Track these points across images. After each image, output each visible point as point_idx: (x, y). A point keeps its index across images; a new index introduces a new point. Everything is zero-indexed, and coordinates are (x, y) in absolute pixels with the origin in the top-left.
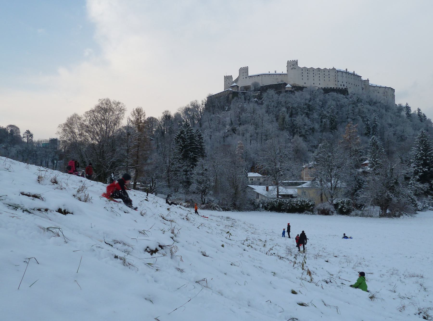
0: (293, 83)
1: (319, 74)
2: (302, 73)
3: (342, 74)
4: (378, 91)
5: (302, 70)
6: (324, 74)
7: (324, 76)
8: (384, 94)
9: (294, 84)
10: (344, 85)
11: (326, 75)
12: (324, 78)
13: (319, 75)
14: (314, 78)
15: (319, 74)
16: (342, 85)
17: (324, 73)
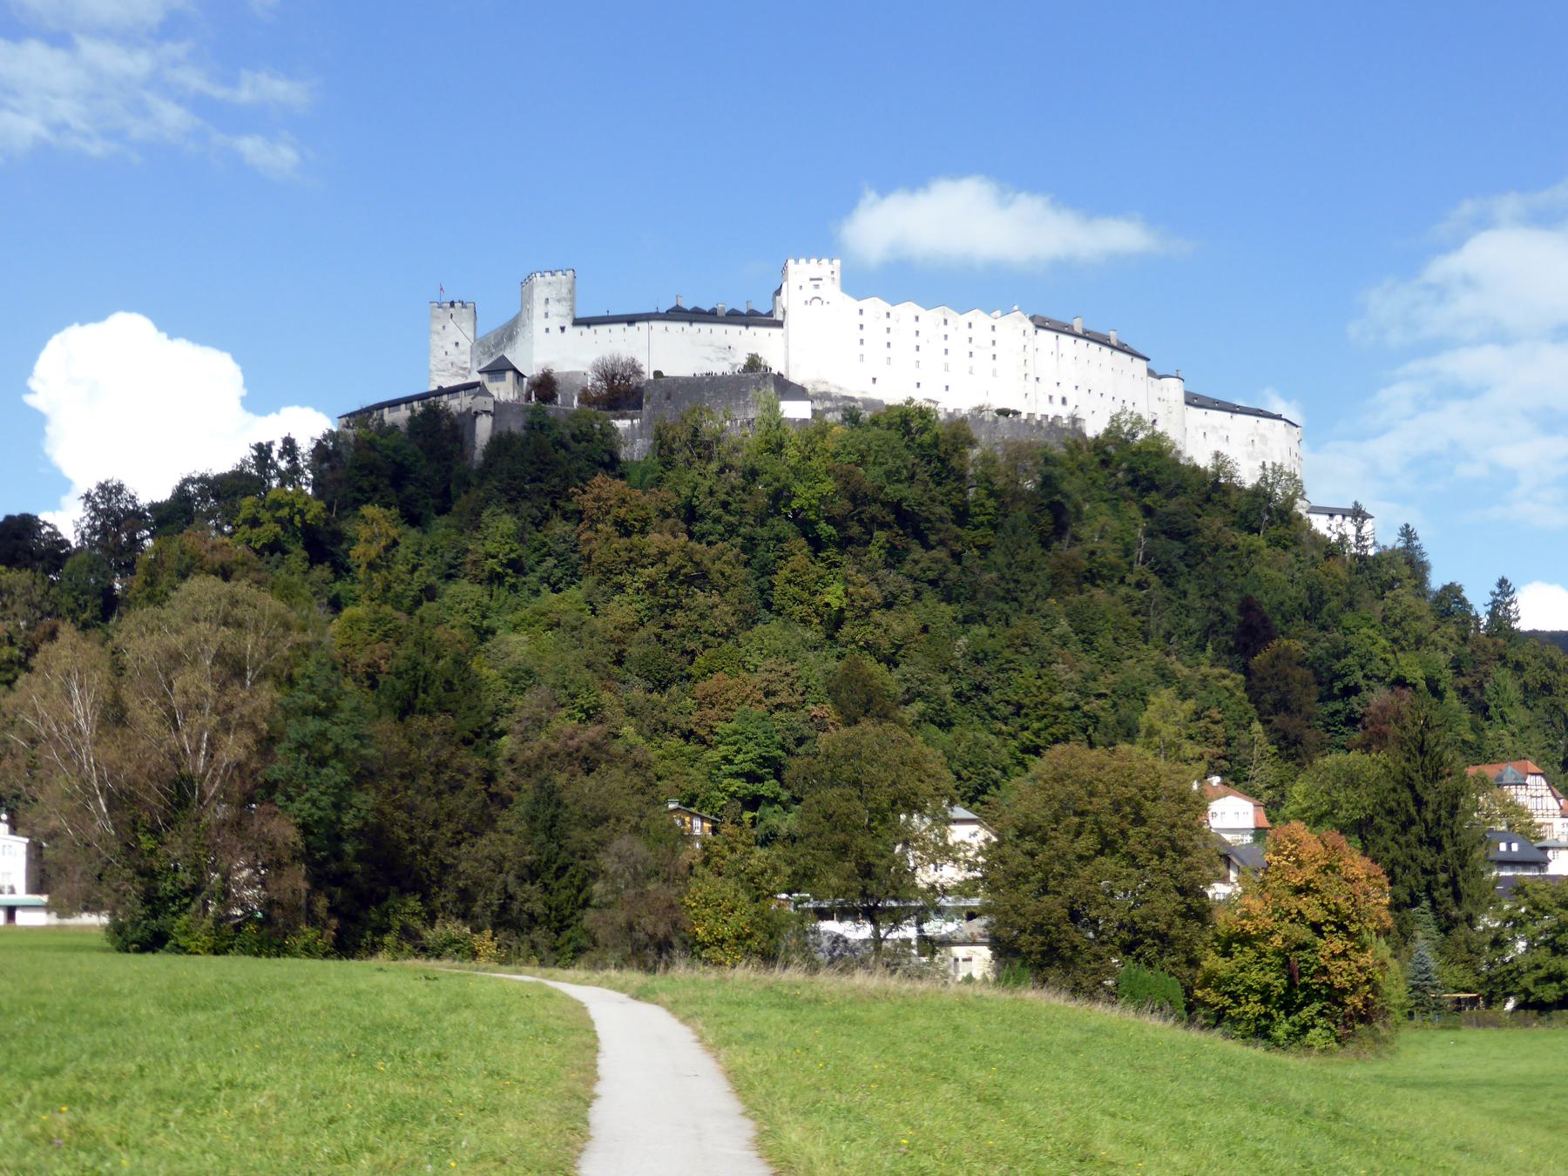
7: (971, 347)
8: (1250, 448)
9: (817, 382)
10: (1064, 401)
11: (978, 347)
16: (1057, 400)
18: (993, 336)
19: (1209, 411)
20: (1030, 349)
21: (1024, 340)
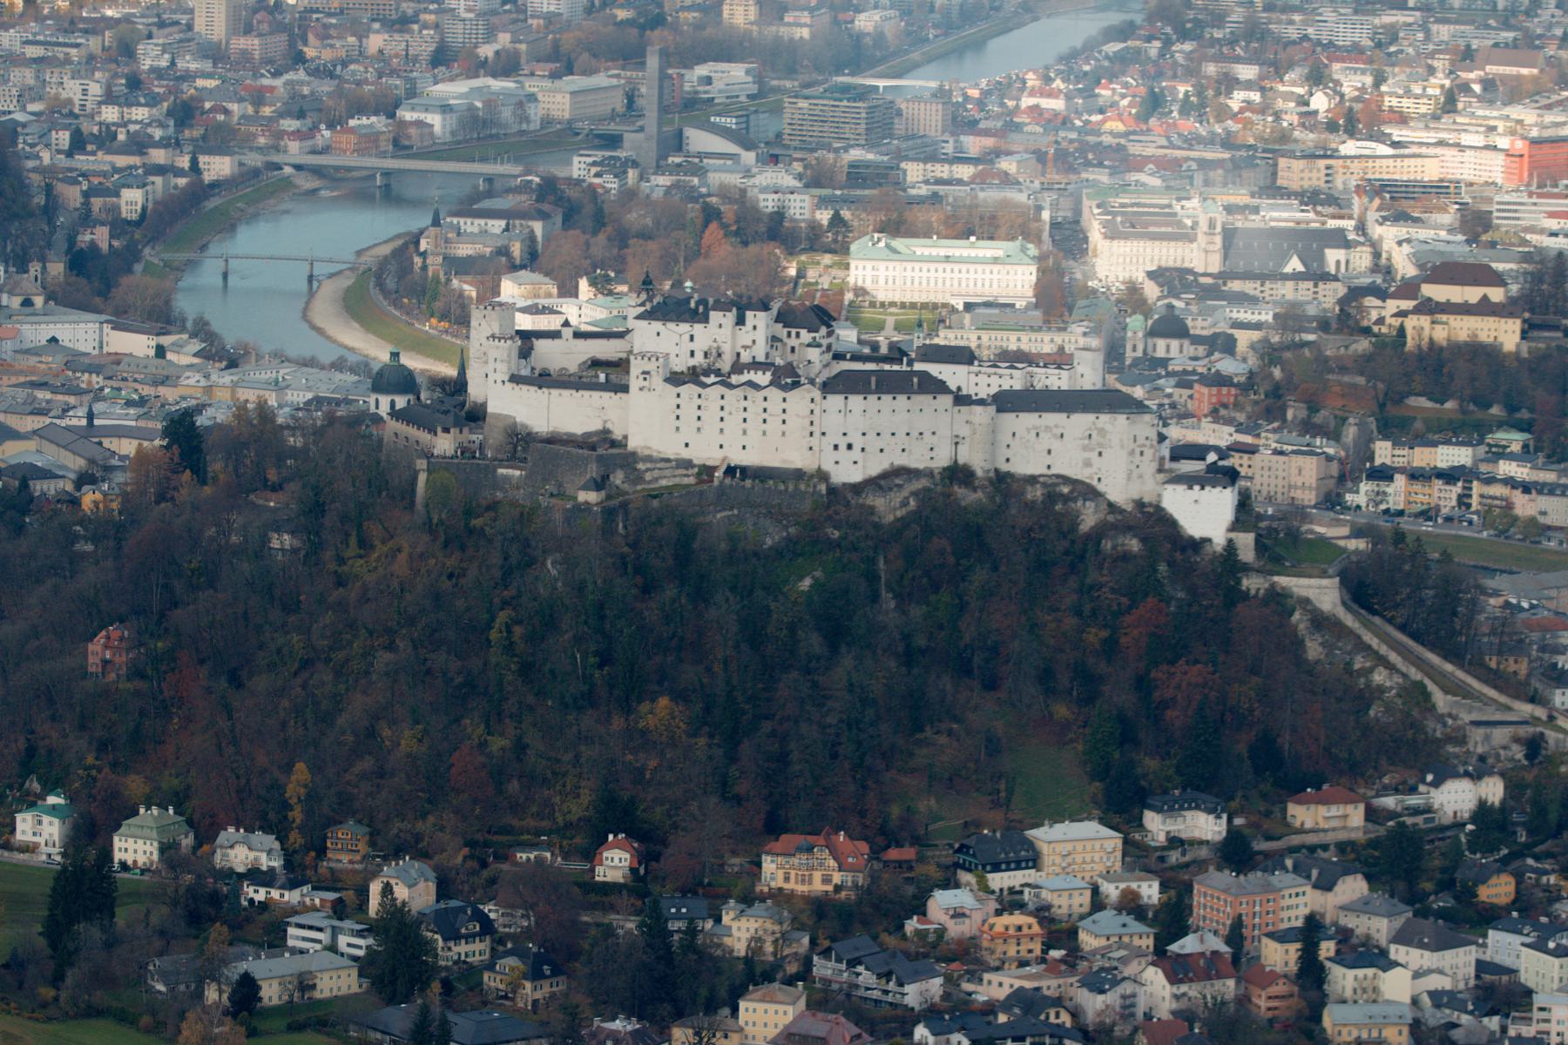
0: (642, 443)
1: (745, 409)
2: (678, 406)
3: (846, 405)
4: (1058, 432)
5: (678, 395)
6: (765, 410)
8: (1086, 442)
10: (850, 447)
12: (764, 426)
13: (745, 415)
14: (722, 425)
15: (745, 409)
16: (843, 447)
17: (765, 405)
18: (784, 405)
19: (1044, 415)
20: (817, 412)
21: (812, 406)
